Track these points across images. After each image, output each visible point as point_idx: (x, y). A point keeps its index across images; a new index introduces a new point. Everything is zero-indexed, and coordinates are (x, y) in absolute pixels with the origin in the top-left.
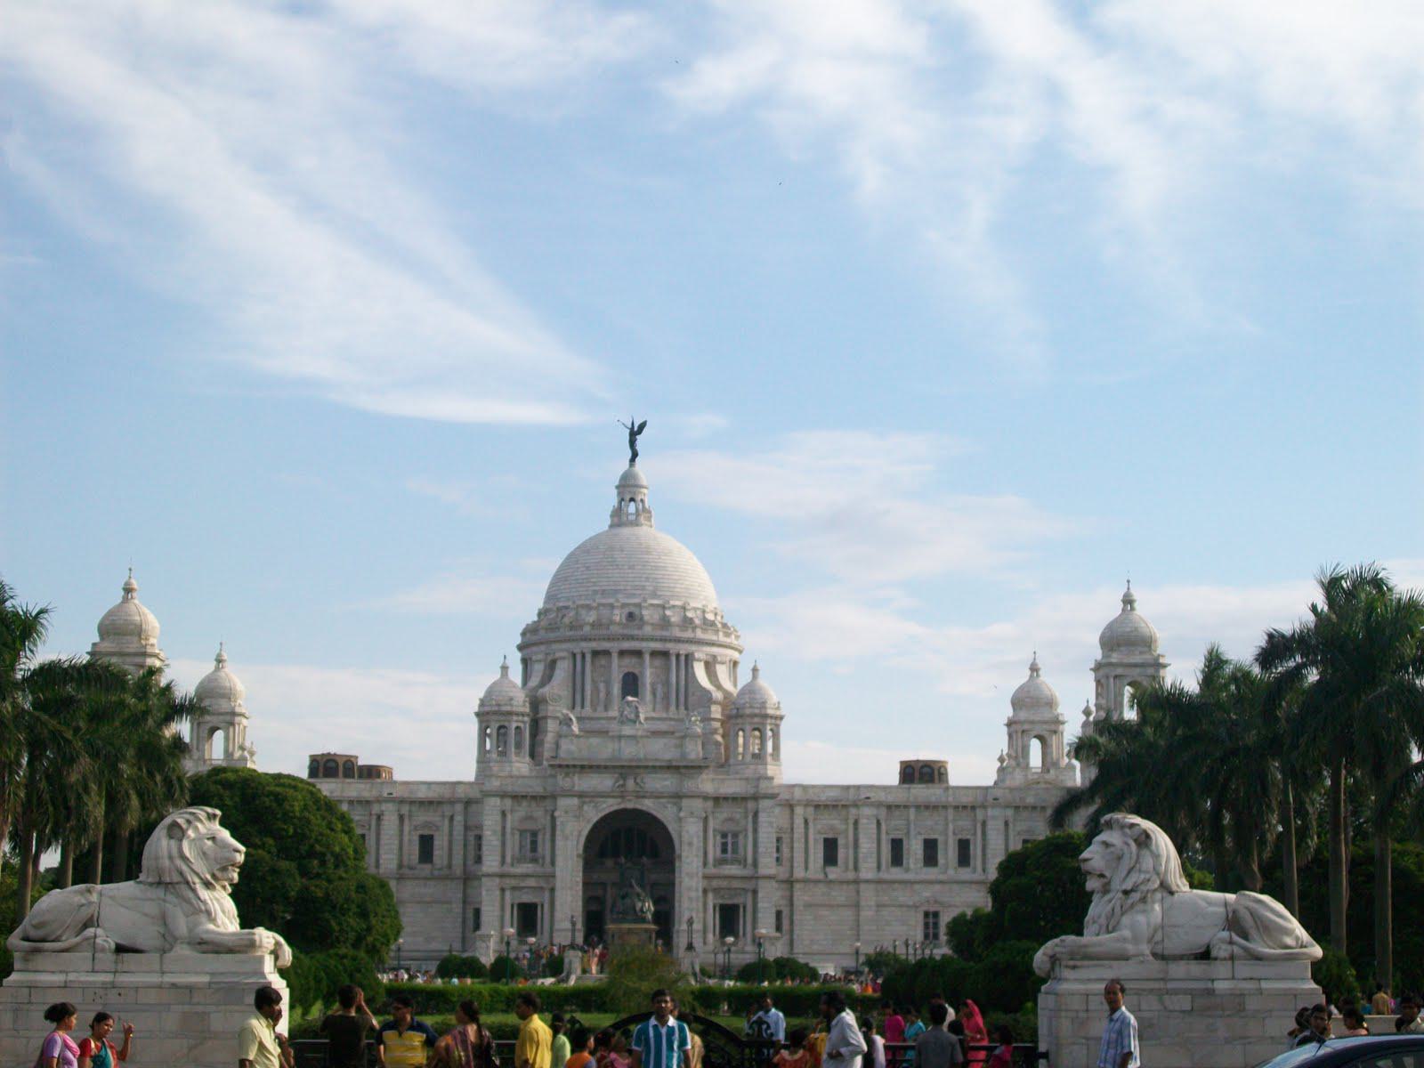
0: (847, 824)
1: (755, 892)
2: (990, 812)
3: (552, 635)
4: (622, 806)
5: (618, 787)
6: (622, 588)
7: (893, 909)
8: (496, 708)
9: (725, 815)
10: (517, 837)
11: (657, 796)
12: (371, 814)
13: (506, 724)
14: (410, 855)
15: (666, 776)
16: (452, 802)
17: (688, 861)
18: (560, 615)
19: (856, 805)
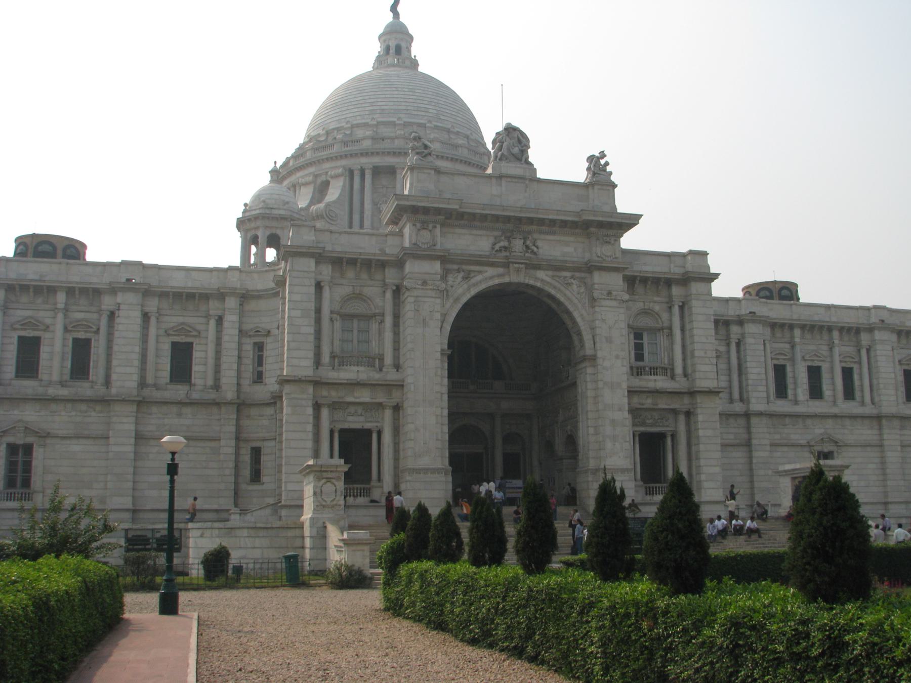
0: (728, 345)
1: (688, 414)
2: (878, 335)
3: (324, 154)
4: (506, 280)
5: (500, 251)
6: (404, 108)
7: (786, 449)
8: (268, 211)
9: (640, 305)
10: (338, 325)
11: (556, 267)
12: (99, 312)
13: (279, 232)
14: (157, 370)
15: (566, 238)
16: (221, 296)
17: (607, 364)
18: (330, 139)
19: (740, 322)
